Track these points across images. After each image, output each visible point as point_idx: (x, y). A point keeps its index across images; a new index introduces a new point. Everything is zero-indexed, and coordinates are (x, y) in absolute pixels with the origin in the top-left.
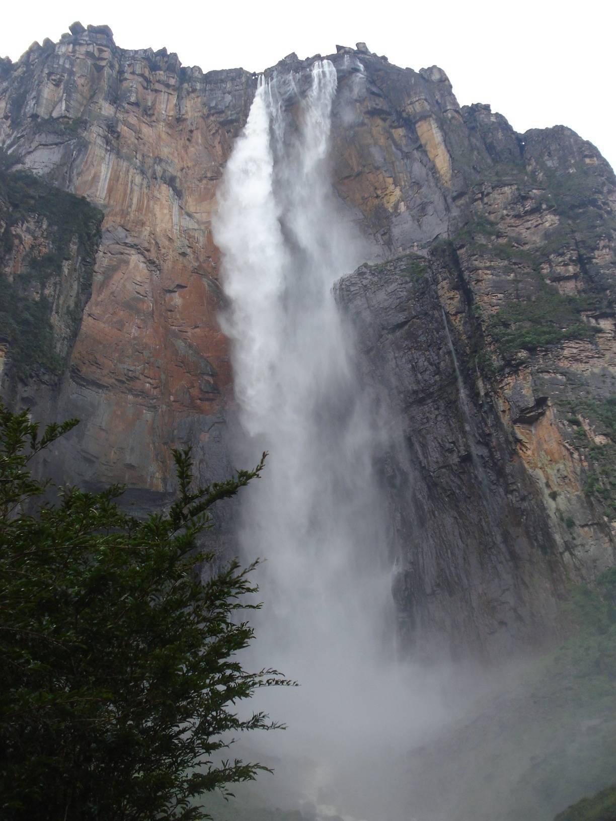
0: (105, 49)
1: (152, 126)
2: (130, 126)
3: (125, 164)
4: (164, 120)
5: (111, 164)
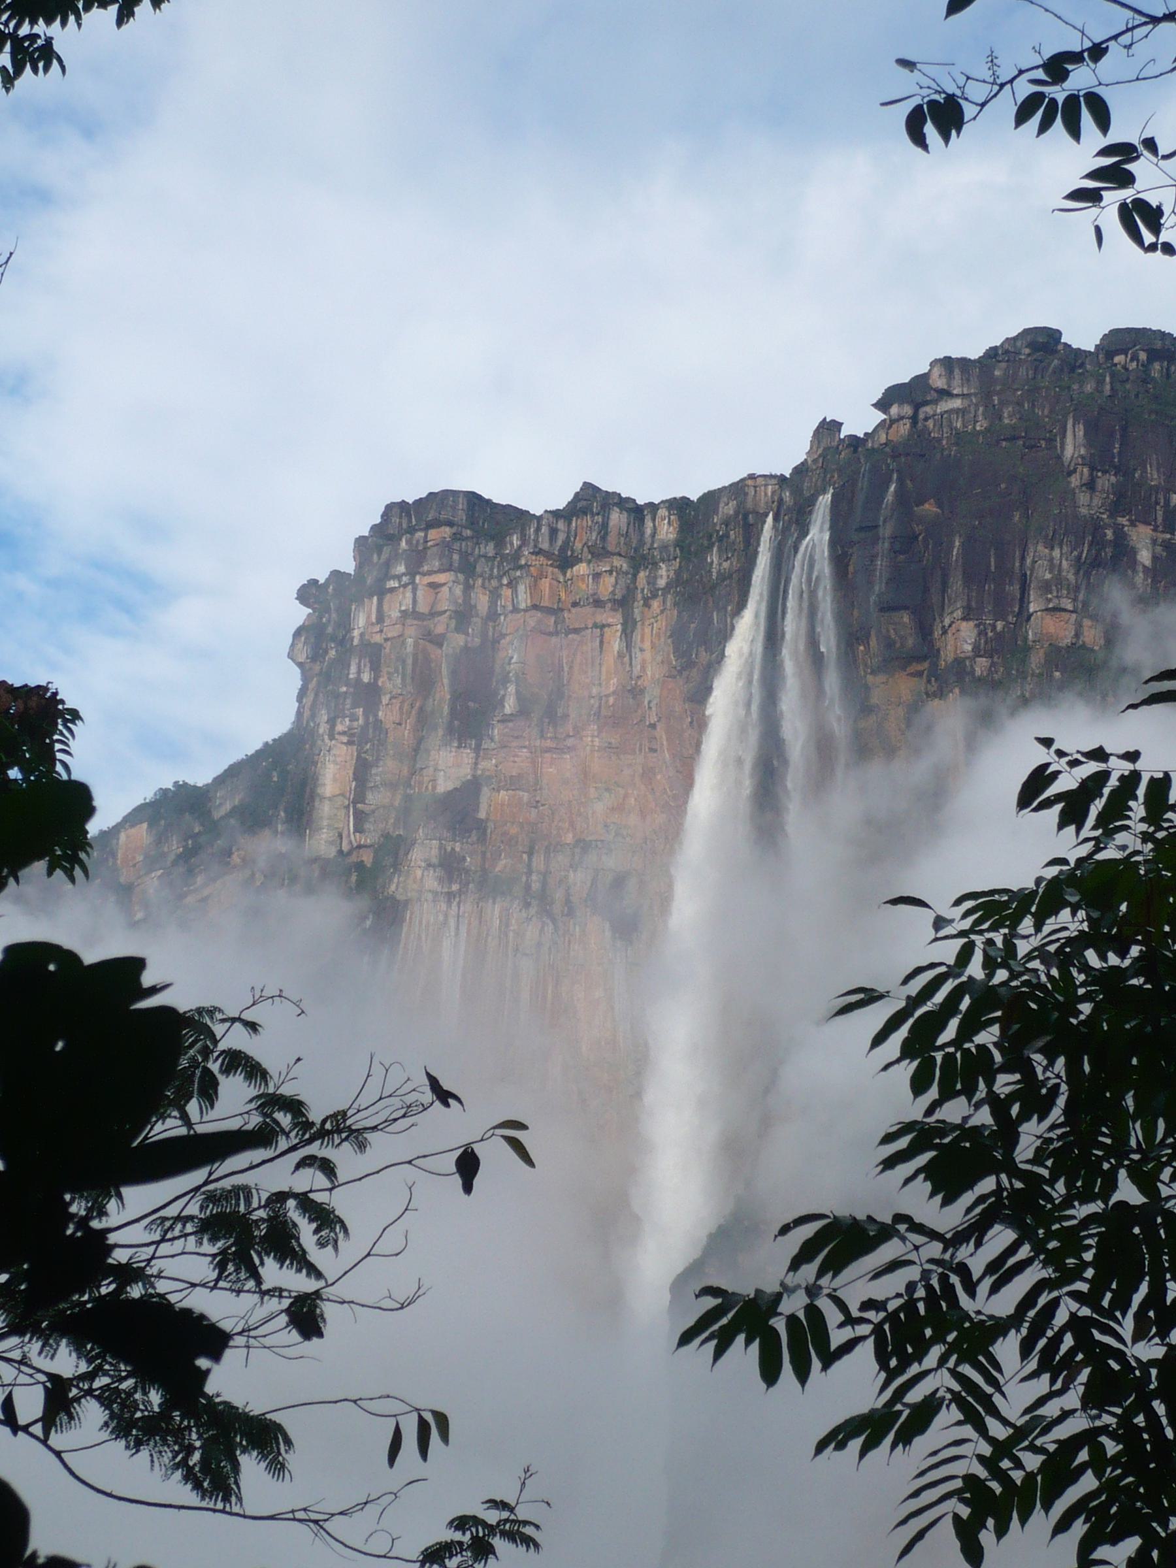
0: (441, 578)
1: (570, 749)
2: (513, 783)
3: (494, 910)
4: (598, 714)
5: (463, 930)
